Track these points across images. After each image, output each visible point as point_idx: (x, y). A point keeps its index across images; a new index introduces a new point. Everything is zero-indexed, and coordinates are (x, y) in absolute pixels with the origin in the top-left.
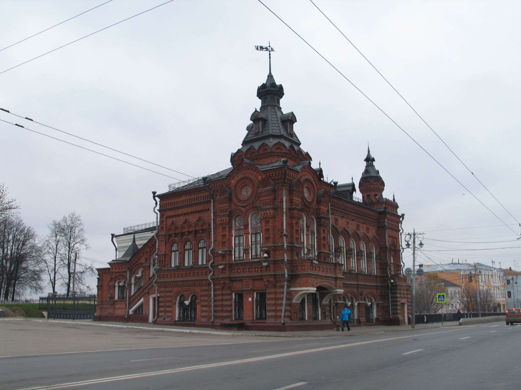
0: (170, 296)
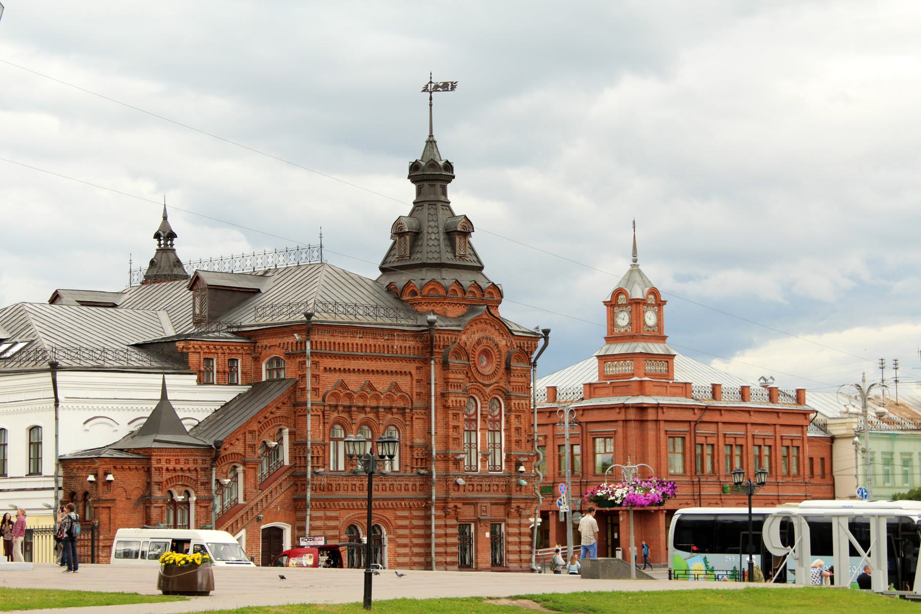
0: (335, 528)
